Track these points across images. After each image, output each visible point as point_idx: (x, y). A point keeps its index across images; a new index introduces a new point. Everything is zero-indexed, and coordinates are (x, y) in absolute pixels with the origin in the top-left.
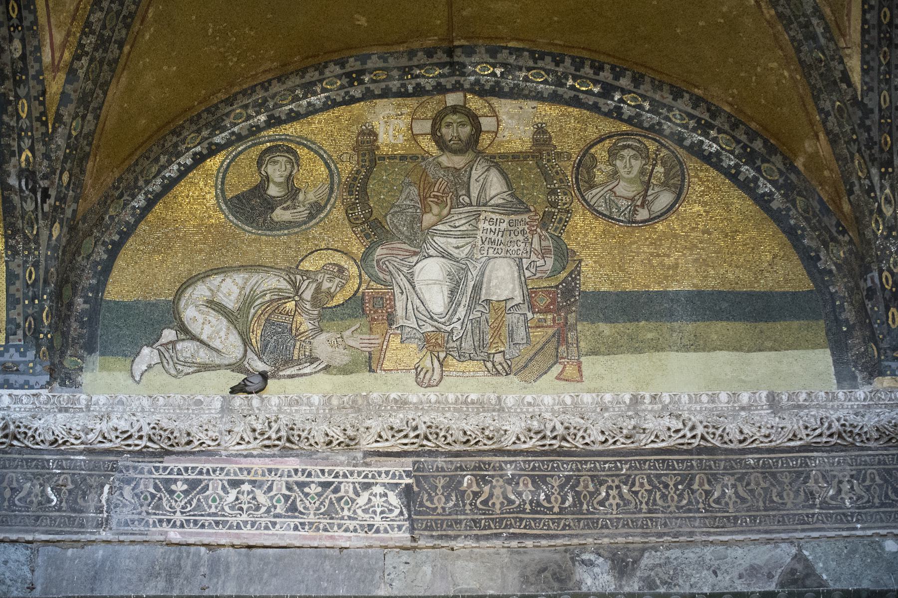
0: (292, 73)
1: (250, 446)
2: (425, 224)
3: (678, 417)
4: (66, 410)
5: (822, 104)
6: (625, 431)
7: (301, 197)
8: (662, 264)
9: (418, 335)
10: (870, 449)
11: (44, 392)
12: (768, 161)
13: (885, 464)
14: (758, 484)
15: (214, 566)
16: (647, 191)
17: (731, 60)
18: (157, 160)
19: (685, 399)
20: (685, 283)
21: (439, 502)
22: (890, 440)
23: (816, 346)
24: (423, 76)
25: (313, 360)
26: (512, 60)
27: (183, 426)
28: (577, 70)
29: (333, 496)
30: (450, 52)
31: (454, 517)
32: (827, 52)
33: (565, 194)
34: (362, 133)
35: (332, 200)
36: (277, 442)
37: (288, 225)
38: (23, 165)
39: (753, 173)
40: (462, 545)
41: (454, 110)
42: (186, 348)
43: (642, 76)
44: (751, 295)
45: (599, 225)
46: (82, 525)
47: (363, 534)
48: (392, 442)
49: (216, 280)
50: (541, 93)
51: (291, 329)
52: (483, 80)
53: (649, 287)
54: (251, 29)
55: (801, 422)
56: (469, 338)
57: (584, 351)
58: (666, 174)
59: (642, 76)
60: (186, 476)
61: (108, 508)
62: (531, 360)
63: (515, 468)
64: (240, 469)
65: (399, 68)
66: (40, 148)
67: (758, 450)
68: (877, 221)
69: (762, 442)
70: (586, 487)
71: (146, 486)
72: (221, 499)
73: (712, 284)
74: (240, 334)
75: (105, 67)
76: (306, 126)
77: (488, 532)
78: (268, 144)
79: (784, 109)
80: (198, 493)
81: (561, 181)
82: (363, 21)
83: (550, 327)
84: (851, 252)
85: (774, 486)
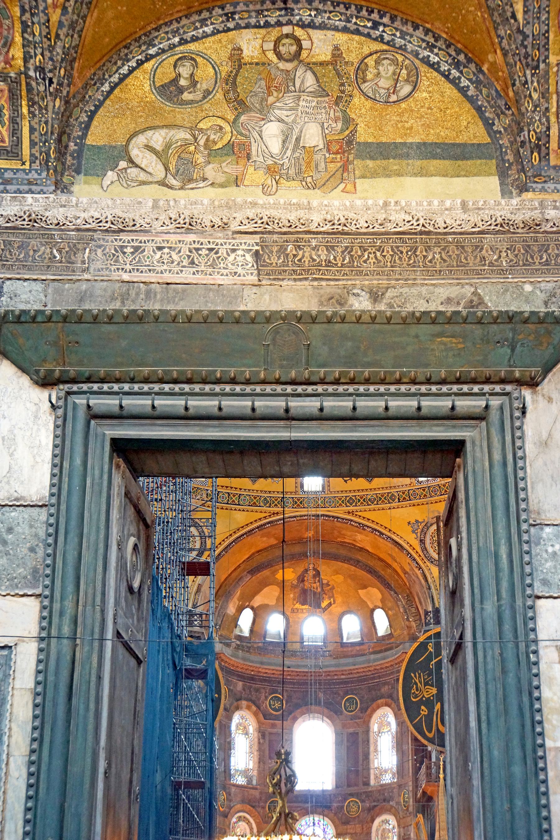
0: (193, 13)
1: (168, 227)
2: (269, 102)
3: (409, 213)
4: (65, 206)
5: (499, 32)
6: (379, 222)
7: (199, 86)
8: (403, 127)
9: (264, 166)
10: (518, 233)
11: (52, 196)
12: (467, 67)
13: (527, 242)
14: (454, 252)
15: (148, 293)
16: (396, 84)
17: (447, 6)
18: (116, 63)
19: (414, 204)
20: (417, 137)
21: (274, 260)
22: (530, 228)
23: (490, 174)
25: (204, 179)
26: (321, 6)
27: (131, 216)
28: (358, 12)
29: (215, 256)
31: (282, 268)
33: (349, 86)
34: (234, 49)
35: (216, 88)
36: (184, 226)
37: (192, 102)
39: (458, 74)
41: (287, 36)
42: (133, 172)
43: (396, 16)
44: (454, 145)
45: (369, 104)
46: (74, 271)
47: (231, 277)
48: (248, 226)
49: (150, 133)
50: (338, 26)
53: (395, 140)
55: (479, 218)
56: (293, 168)
57: (357, 176)
58: (408, 74)
59: (396, 16)
60: (132, 244)
61: (89, 261)
62: (328, 180)
63: (317, 242)
64: (163, 240)
65: (256, 11)
66: (47, 54)
67: (454, 233)
68: (528, 102)
70: (357, 252)
71: (110, 250)
72: (152, 257)
73: (432, 139)
75: (84, 6)
76: (201, 45)
77: (301, 277)
78: (180, 55)
79: (478, 36)
81: (347, 78)
84: (512, 120)
85: (462, 253)
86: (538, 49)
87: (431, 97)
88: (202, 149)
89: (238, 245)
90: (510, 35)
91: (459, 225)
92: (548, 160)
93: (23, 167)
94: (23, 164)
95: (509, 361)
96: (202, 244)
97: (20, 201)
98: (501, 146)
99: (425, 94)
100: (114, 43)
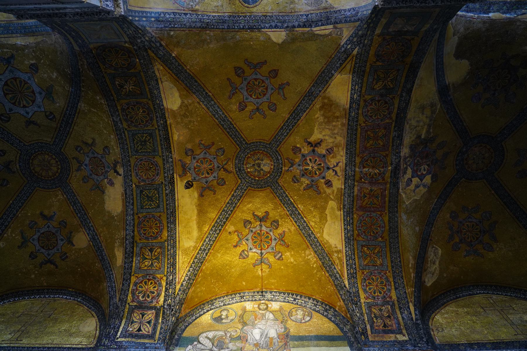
5: (340, 293)
7: (229, 318)
8: (308, 330)
18: (199, 310)
23: (345, 346)
26: (275, 294)
30: (262, 292)
39: (327, 314)
41: (263, 303)
42: (199, 346)
43: (302, 295)
44: (329, 336)
45: (294, 323)
49: (208, 333)
56: (265, 345)
58: (308, 314)
59: (302, 295)
66: (173, 300)
73: (319, 334)
79: (333, 297)
82: (244, 283)
90: (344, 293)
92: (368, 338)
94: (155, 341)
98: (348, 336)
100: (199, 302)
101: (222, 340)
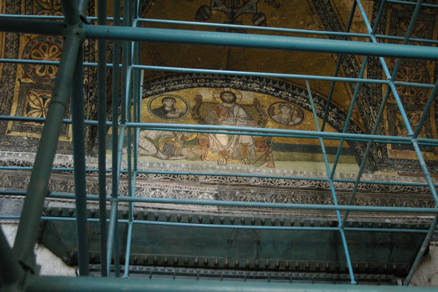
0: (175, 75)
1: (160, 178)
2: (219, 121)
4: (93, 163)
7: (177, 111)
10: (376, 192)
12: (332, 111)
13: (382, 197)
16: (292, 117)
24: (217, 83)
25: (181, 155)
28: (267, 83)
29: (189, 195)
32: (355, 69)
33: (265, 116)
34: (197, 96)
35: (187, 113)
37: (173, 118)
38: (84, 83)
40: (237, 212)
41: (227, 92)
43: (289, 85)
48: (211, 179)
51: (174, 146)
52: (236, 85)
54: (163, 55)
58: (298, 113)
64: (156, 185)
66: (91, 79)
69: (339, 188)
70: (280, 197)
71: (121, 188)
74: (156, 147)
78: (166, 96)
80: (140, 191)
81: (263, 113)
83: (262, 152)
86: (376, 96)
87: (312, 124)
88: (180, 140)
89: (204, 190)
91: (341, 186)
92: (387, 155)
93: (68, 140)
94: (69, 138)
95: (389, 258)
96: (181, 188)
97: (64, 159)
98: (357, 150)
99: (309, 123)
101: (170, 143)
